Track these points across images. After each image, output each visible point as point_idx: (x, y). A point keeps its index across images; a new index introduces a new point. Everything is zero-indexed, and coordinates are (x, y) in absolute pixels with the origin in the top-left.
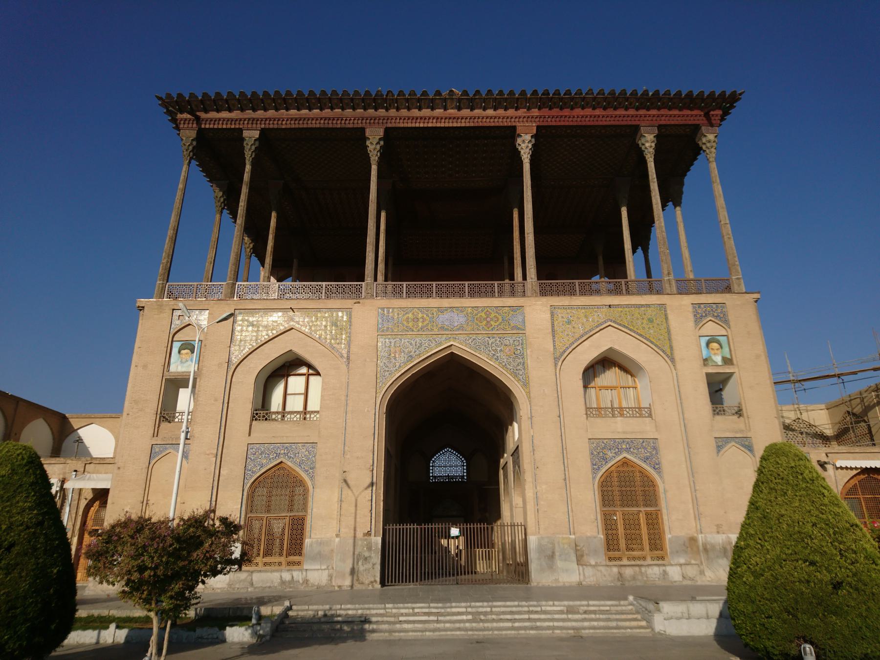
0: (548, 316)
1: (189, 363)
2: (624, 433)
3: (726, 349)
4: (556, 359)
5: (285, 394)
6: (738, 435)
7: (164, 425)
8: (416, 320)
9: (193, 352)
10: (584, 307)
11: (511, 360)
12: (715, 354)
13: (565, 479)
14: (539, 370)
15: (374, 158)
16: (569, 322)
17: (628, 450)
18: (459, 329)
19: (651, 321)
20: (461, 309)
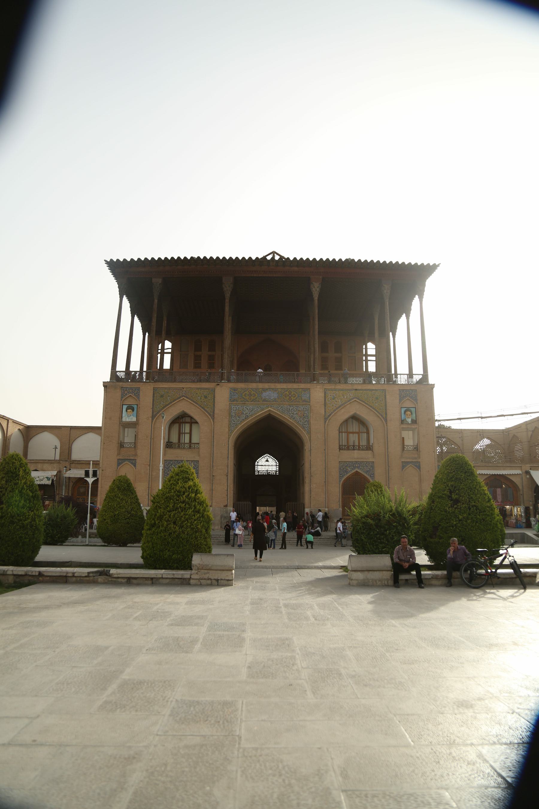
0: (322, 395)
1: (132, 416)
2: (357, 458)
3: (414, 415)
4: (326, 419)
5: (180, 434)
6: (413, 461)
7: (122, 449)
8: (250, 395)
9: (133, 410)
10: (342, 390)
11: (301, 419)
12: (408, 418)
13: (325, 482)
14: (317, 425)
15: (228, 295)
16: (334, 399)
17: (358, 467)
18: (273, 401)
19: (377, 399)
20: (275, 390)
